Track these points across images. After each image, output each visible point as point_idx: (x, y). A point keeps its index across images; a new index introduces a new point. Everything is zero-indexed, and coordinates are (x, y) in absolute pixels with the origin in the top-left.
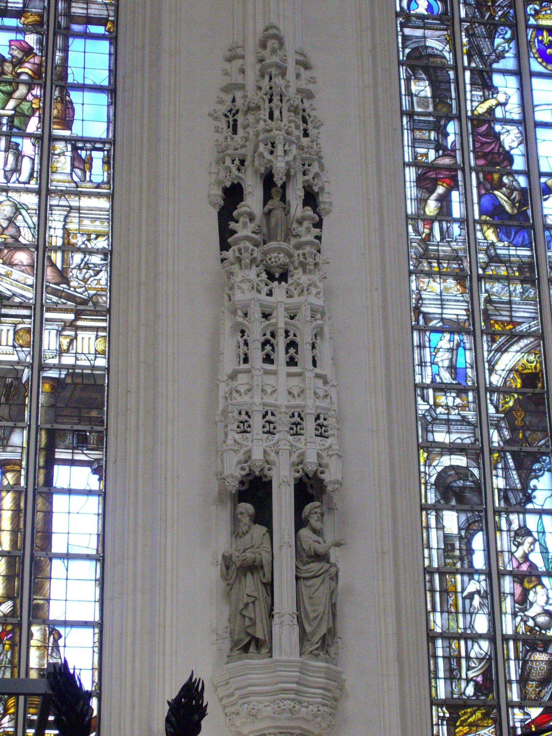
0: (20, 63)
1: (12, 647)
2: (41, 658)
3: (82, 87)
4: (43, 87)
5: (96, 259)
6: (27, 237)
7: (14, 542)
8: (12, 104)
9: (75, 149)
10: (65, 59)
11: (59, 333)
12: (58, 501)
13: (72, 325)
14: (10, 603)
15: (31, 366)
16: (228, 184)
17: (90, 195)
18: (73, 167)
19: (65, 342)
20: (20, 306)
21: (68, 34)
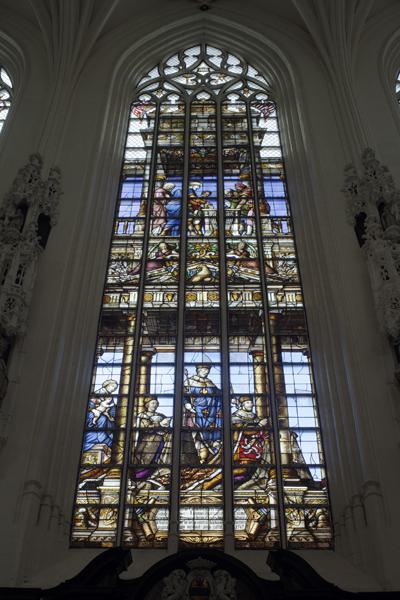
0: (241, 192)
1: (269, 442)
2: (287, 448)
3: (273, 198)
4: (253, 199)
5: (290, 263)
6: (253, 256)
7: (264, 389)
8: (239, 206)
9: (272, 221)
10: (263, 189)
11: (276, 294)
12: (287, 370)
13: (282, 290)
14: (266, 420)
15: (262, 308)
16: (358, 213)
17: (283, 238)
18: (273, 228)
19: (279, 298)
20: (253, 283)
21: (263, 180)
